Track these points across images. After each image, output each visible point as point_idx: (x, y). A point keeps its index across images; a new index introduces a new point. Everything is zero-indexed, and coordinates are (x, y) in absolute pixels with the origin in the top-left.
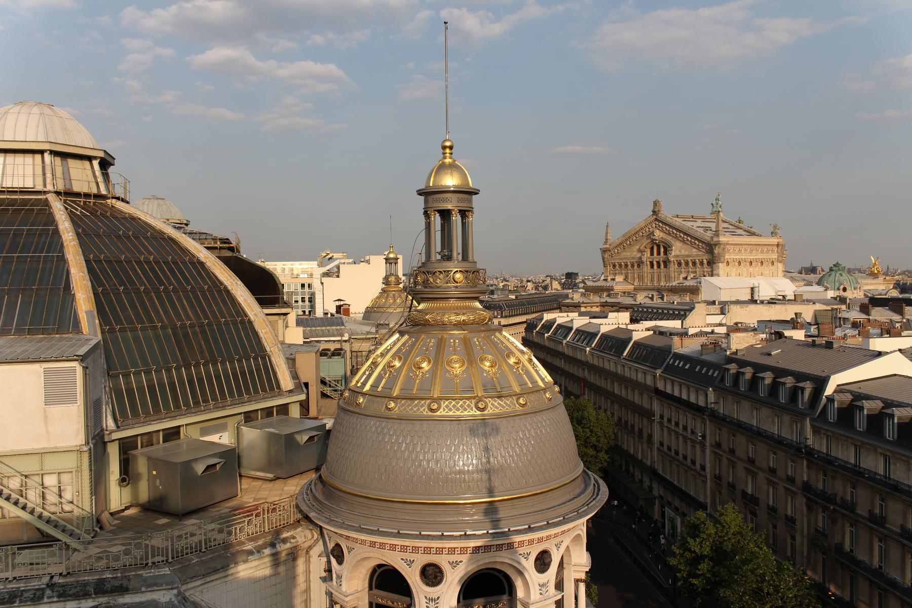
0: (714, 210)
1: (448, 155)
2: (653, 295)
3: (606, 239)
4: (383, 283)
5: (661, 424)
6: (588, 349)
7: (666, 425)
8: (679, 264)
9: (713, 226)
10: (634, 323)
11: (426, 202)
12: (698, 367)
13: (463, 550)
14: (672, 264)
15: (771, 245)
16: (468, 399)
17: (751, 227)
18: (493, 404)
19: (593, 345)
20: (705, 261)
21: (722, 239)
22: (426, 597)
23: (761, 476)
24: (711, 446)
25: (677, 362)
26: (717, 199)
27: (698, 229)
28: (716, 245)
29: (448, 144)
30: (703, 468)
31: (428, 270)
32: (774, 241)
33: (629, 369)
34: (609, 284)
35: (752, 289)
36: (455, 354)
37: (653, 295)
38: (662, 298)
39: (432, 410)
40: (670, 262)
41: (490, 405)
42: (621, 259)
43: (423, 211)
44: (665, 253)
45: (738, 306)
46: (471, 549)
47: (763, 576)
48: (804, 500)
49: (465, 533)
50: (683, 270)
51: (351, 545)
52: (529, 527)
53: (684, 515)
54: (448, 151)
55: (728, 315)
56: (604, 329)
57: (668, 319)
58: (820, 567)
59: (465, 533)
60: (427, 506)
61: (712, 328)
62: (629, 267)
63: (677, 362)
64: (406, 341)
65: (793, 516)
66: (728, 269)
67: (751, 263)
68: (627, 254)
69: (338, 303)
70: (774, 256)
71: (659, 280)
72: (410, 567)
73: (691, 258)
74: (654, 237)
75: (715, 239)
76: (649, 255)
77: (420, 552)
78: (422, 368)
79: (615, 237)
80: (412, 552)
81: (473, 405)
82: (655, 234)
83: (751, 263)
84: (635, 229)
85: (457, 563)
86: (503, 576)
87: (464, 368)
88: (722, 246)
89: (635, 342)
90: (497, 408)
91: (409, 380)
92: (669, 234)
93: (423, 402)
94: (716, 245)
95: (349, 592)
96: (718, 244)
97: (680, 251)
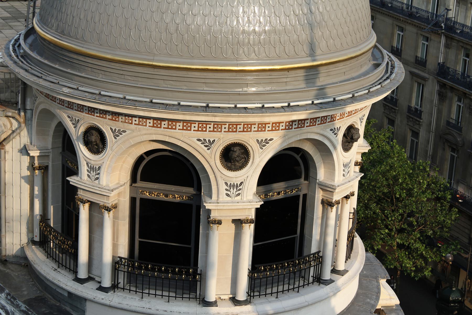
13: (276, 126)
22: (226, 184)
46: (284, 124)
47: (395, 178)
48: (437, 88)
51: (119, 125)
58: (447, 166)
60: (234, 74)
65: (419, 107)
72: (208, 149)
77: (223, 130)
85: (267, 142)
86: (300, 157)
95: (112, 186)
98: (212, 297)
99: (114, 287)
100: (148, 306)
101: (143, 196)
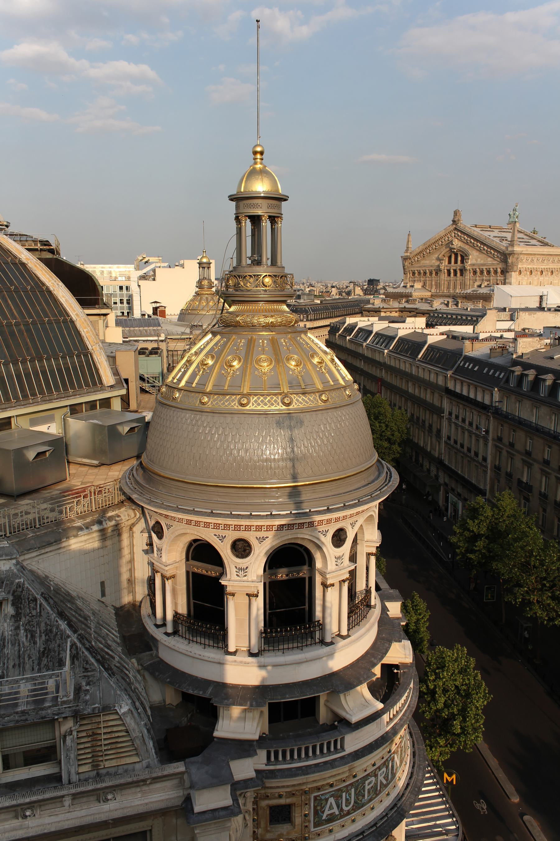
0: (511, 220)
1: (259, 160)
2: (448, 302)
3: (408, 248)
4: (197, 287)
5: (449, 420)
6: (386, 351)
7: (453, 421)
8: (475, 272)
9: (509, 236)
10: (430, 328)
11: (237, 207)
12: (486, 369)
13: (269, 528)
14: (468, 272)
16: (275, 395)
17: (545, 238)
18: (297, 400)
19: (391, 348)
20: (499, 270)
21: (517, 249)
22: (236, 567)
23: (536, 467)
24: (493, 440)
25: (467, 364)
26: (515, 210)
27: (495, 239)
28: (510, 254)
29: (259, 149)
30: (485, 459)
31: (239, 274)
33: (422, 371)
34: (408, 290)
35: (541, 297)
36: (263, 354)
37: (448, 302)
38: (457, 305)
39: (242, 405)
40: (466, 270)
41: (294, 400)
42: (420, 267)
43: (234, 216)
44: (462, 262)
45: (527, 313)
46: (276, 527)
47: (532, 551)
49: (271, 513)
50: (478, 278)
51: (169, 522)
52: (328, 508)
53: (465, 500)
54: (258, 156)
55: (517, 321)
56: (401, 333)
57: (461, 325)
59: (271, 513)
60: (237, 490)
61: (501, 333)
62: (428, 274)
63: (467, 364)
64: (219, 341)
66: (520, 278)
67: (542, 272)
68: (426, 262)
69: (155, 305)
71: (455, 288)
74: (452, 246)
75: (510, 249)
76: (447, 263)
77: (231, 529)
78: (233, 366)
79: (416, 246)
80: (224, 529)
81: (279, 401)
82: (454, 243)
83: (542, 272)
84: (435, 238)
85: (264, 539)
86: (304, 550)
87: (271, 367)
88: (516, 256)
89: (429, 345)
90: (302, 404)
91: (221, 377)
92: (467, 243)
93: (234, 397)
94: (510, 254)
95: (168, 562)
96: (512, 253)
97: (476, 260)
98: (232, 649)
99: (175, 633)
100: (190, 650)
101: (194, 571)
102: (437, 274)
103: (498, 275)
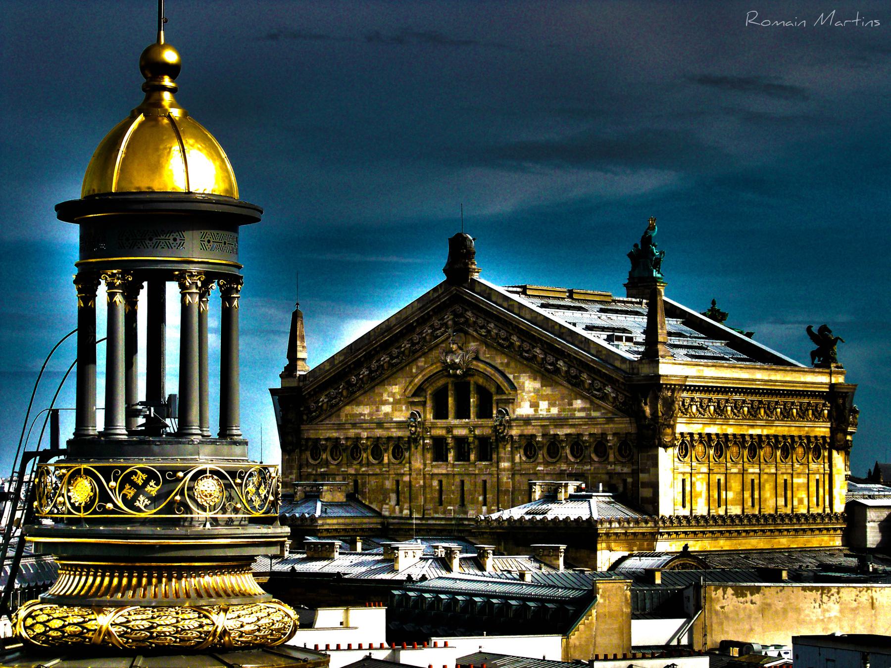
2: (450, 552)
15: (813, 394)
32: (820, 379)
70: (822, 429)
73: (568, 431)
75: (645, 370)
102: (398, 453)
103: (611, 458)
